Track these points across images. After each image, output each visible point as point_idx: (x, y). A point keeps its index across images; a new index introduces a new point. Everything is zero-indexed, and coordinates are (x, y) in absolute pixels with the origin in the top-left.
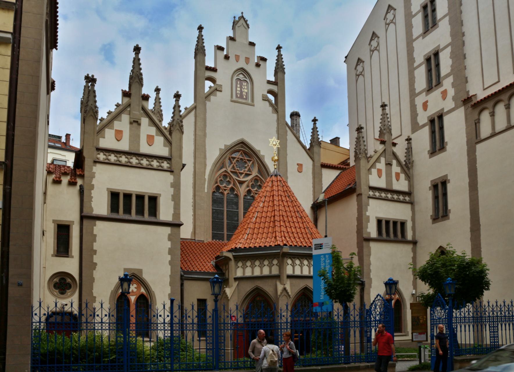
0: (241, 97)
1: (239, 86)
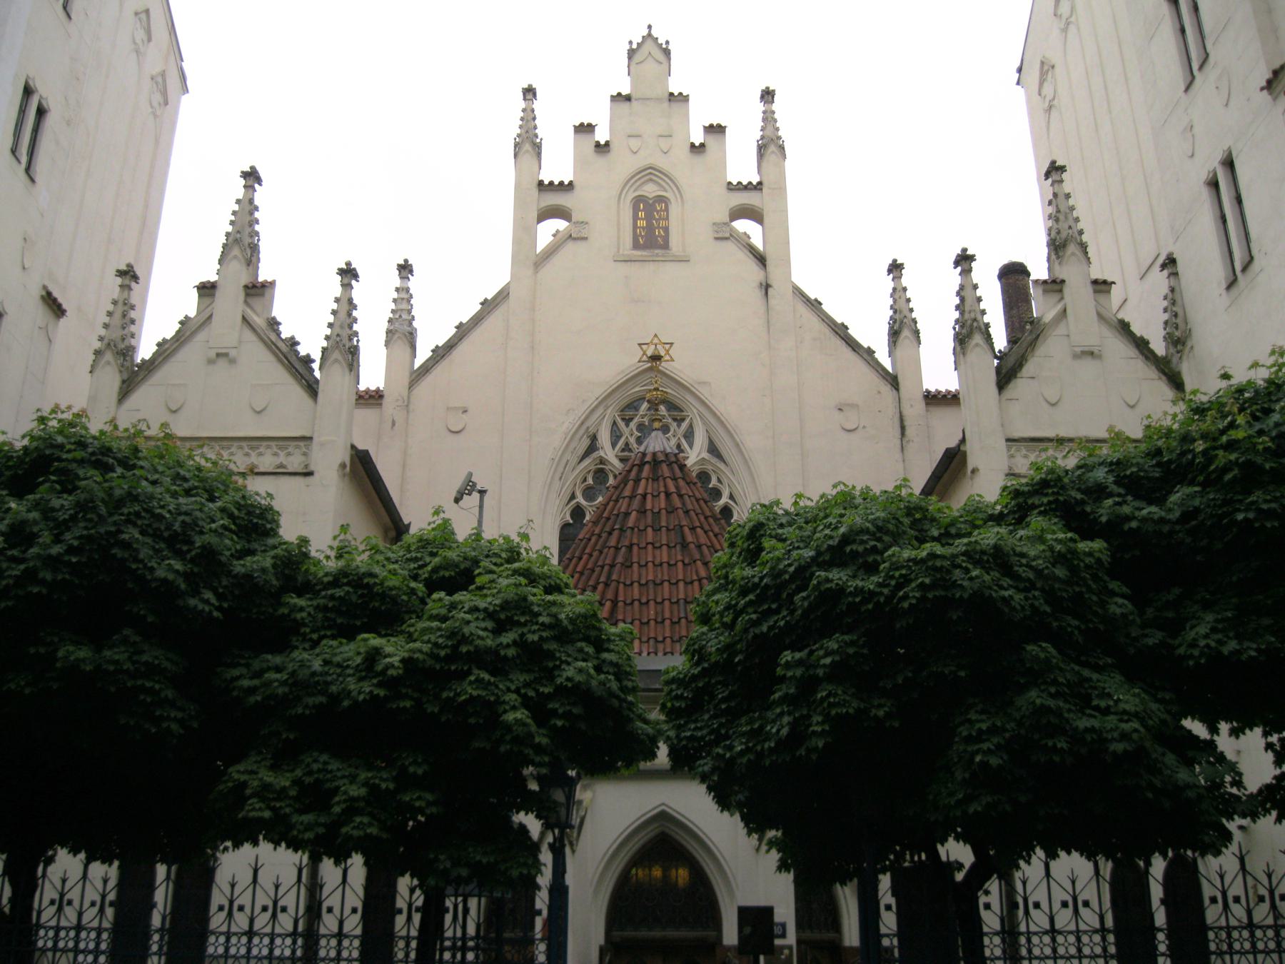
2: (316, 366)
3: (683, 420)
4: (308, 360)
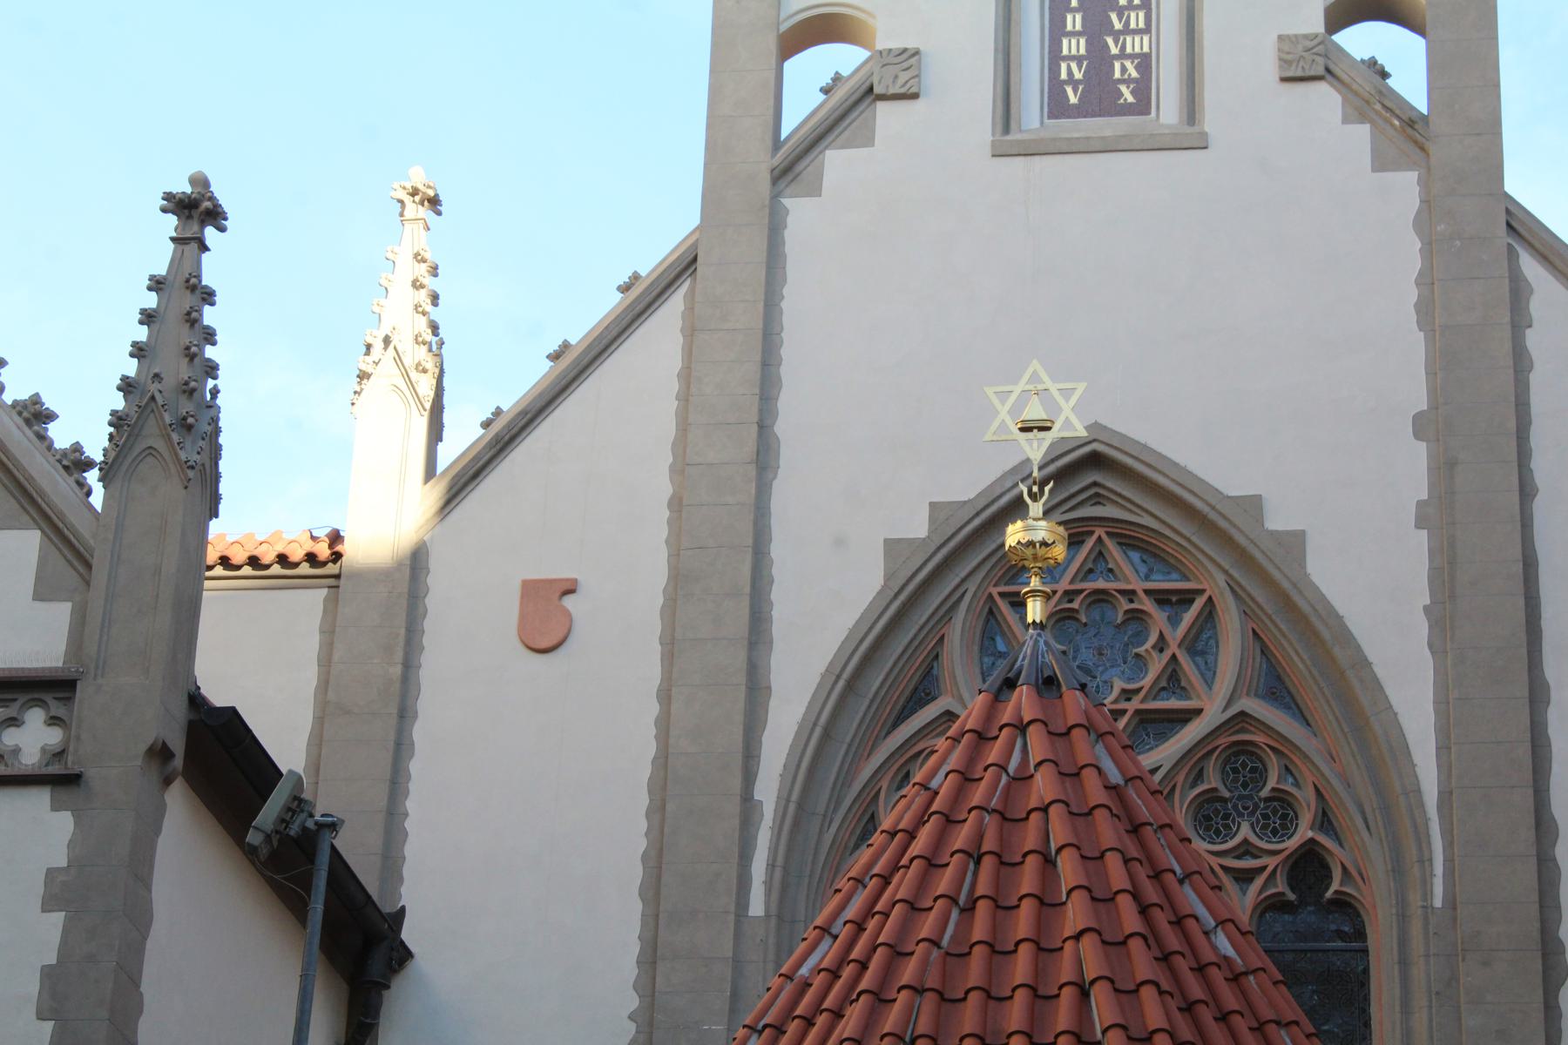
0: (1100, 96)
1: (1074, 22)
2: (92, 477)
3: (1186, 598)
4: (75, 462)
